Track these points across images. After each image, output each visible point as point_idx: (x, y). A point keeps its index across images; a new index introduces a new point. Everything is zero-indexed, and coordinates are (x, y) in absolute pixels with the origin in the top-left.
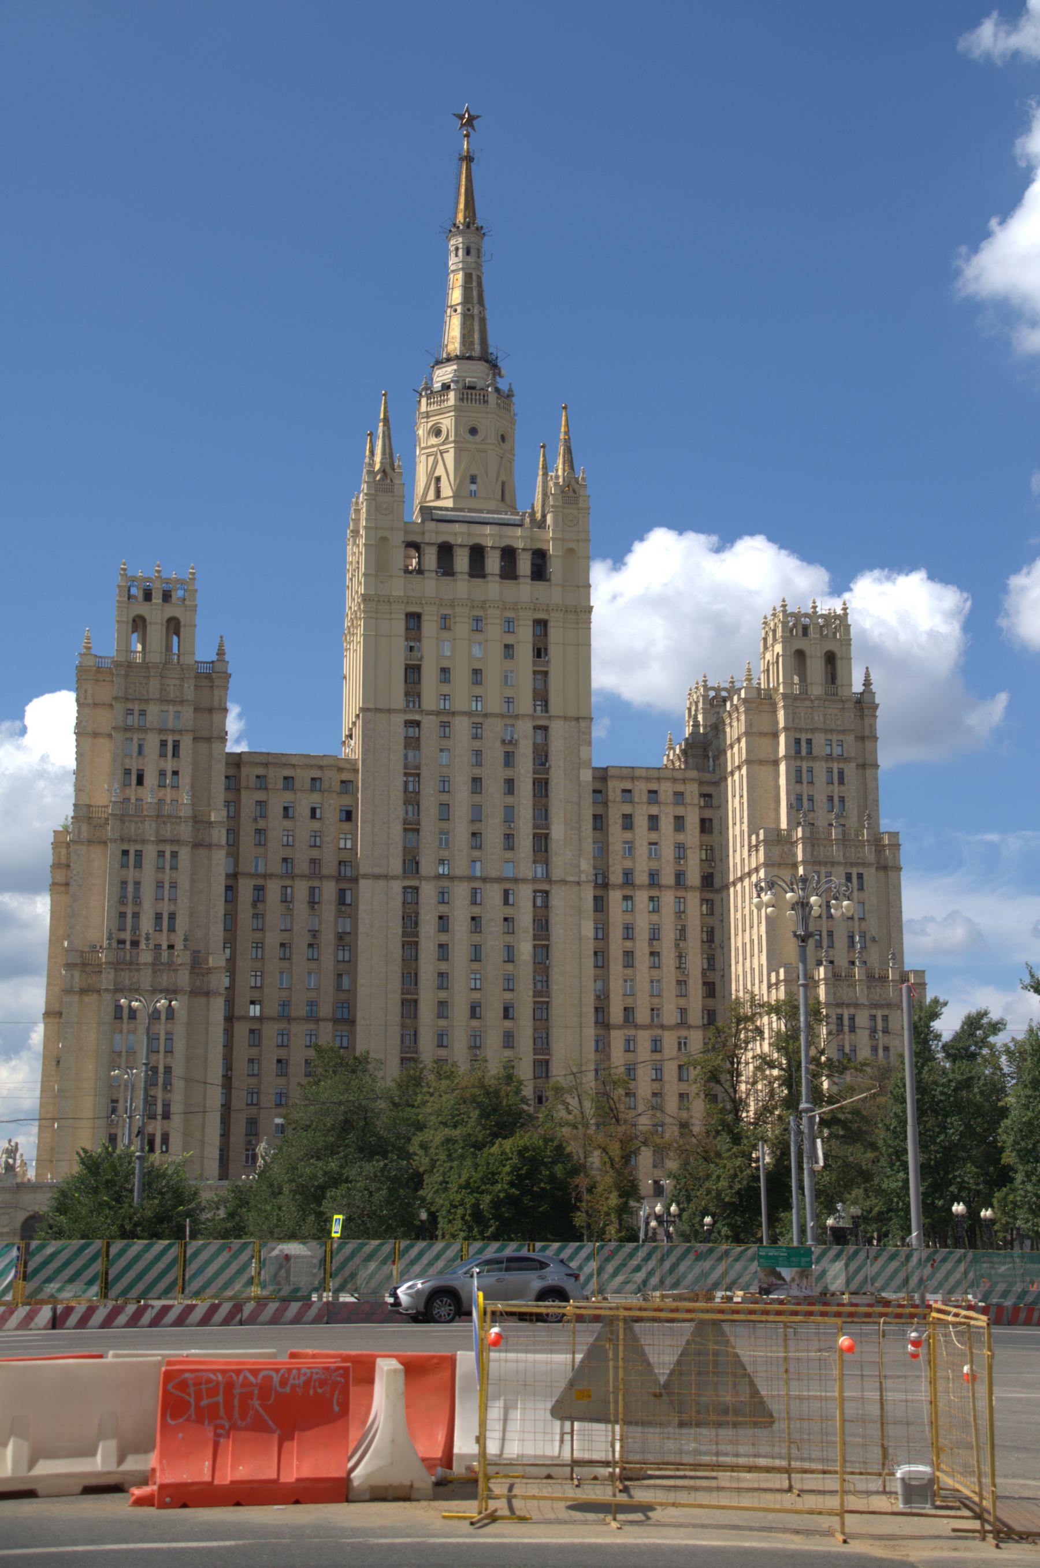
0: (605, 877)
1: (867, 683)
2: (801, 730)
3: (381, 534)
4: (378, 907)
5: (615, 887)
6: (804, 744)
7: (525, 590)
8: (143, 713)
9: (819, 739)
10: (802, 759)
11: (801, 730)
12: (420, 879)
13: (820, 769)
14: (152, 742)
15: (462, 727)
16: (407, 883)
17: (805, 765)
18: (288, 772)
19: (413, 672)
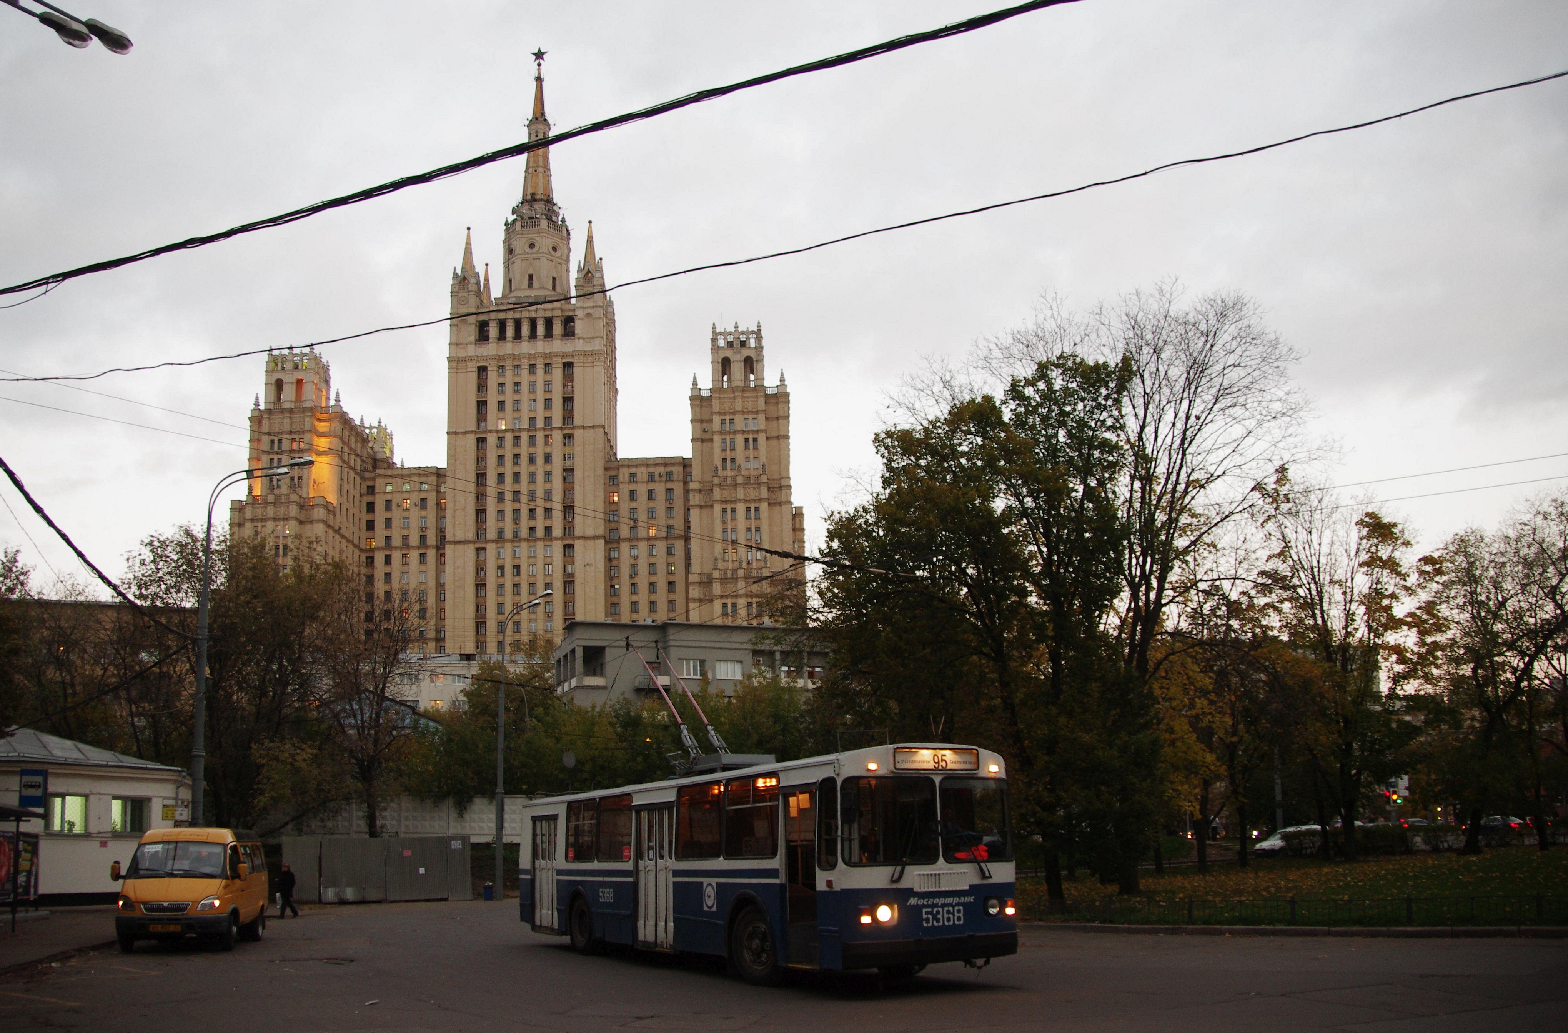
7: (558, 345)
8: (280, 441)
9: (738, 418)
11: (725, 414)
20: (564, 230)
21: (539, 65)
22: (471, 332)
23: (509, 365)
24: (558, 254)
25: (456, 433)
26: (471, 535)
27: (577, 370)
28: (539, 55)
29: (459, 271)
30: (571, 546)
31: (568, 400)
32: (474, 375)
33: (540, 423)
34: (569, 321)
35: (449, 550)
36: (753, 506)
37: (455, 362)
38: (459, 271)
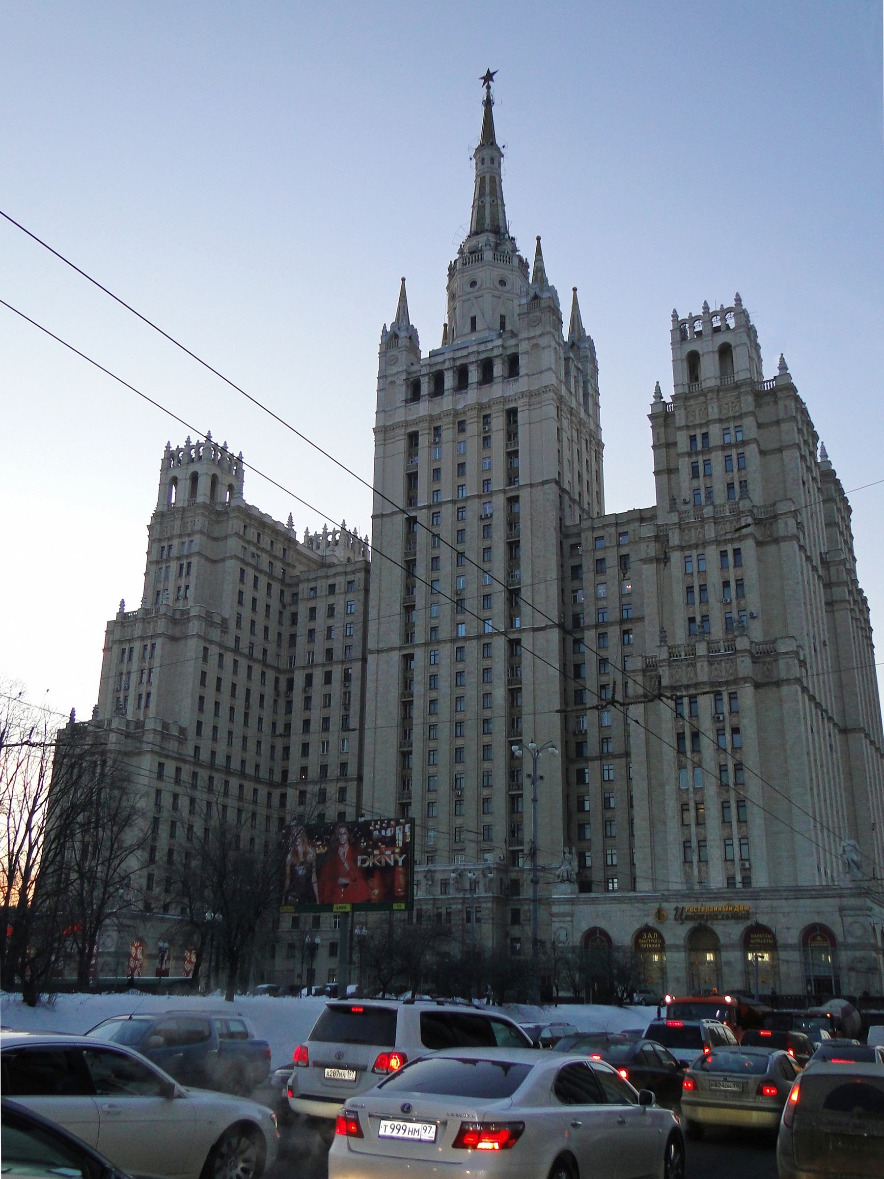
0: (576, 619)
1: (783, 366)
2: (695, 427)
3: (390, 379)
4: (384, 673)
5: (589, 627)
6: (699, 439)
9: (715, 431)
10: (697, 453)
11: (695, 427)
12: (414, 646)
13: (717, 459)
14: (174, 565)
15: (447, 513)
16: (405, 652)
17: (701, 459)
18: (330, 582)
19: (412, 478)
20: (516, 261)
21: (489, 88)
22: (401, 392)
24: (508, 287)
25: (382, 516)
27: (521, 417)
29: (388, 329)
30: (518, 642)
35: (371, 658)
36: (729, 548)
37: (382, 432)
38: (388, 329)
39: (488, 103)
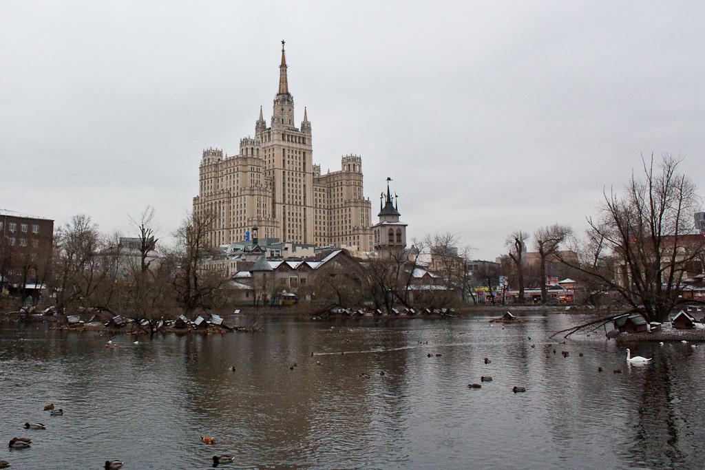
7: (302, 146)
23: (291, 149)
26: (282, 202)
28: (283, 43)
31: (304, 163)
32: (282, 151)
33: (298, 170)
34: (304, 139)
39: (283, 51)
